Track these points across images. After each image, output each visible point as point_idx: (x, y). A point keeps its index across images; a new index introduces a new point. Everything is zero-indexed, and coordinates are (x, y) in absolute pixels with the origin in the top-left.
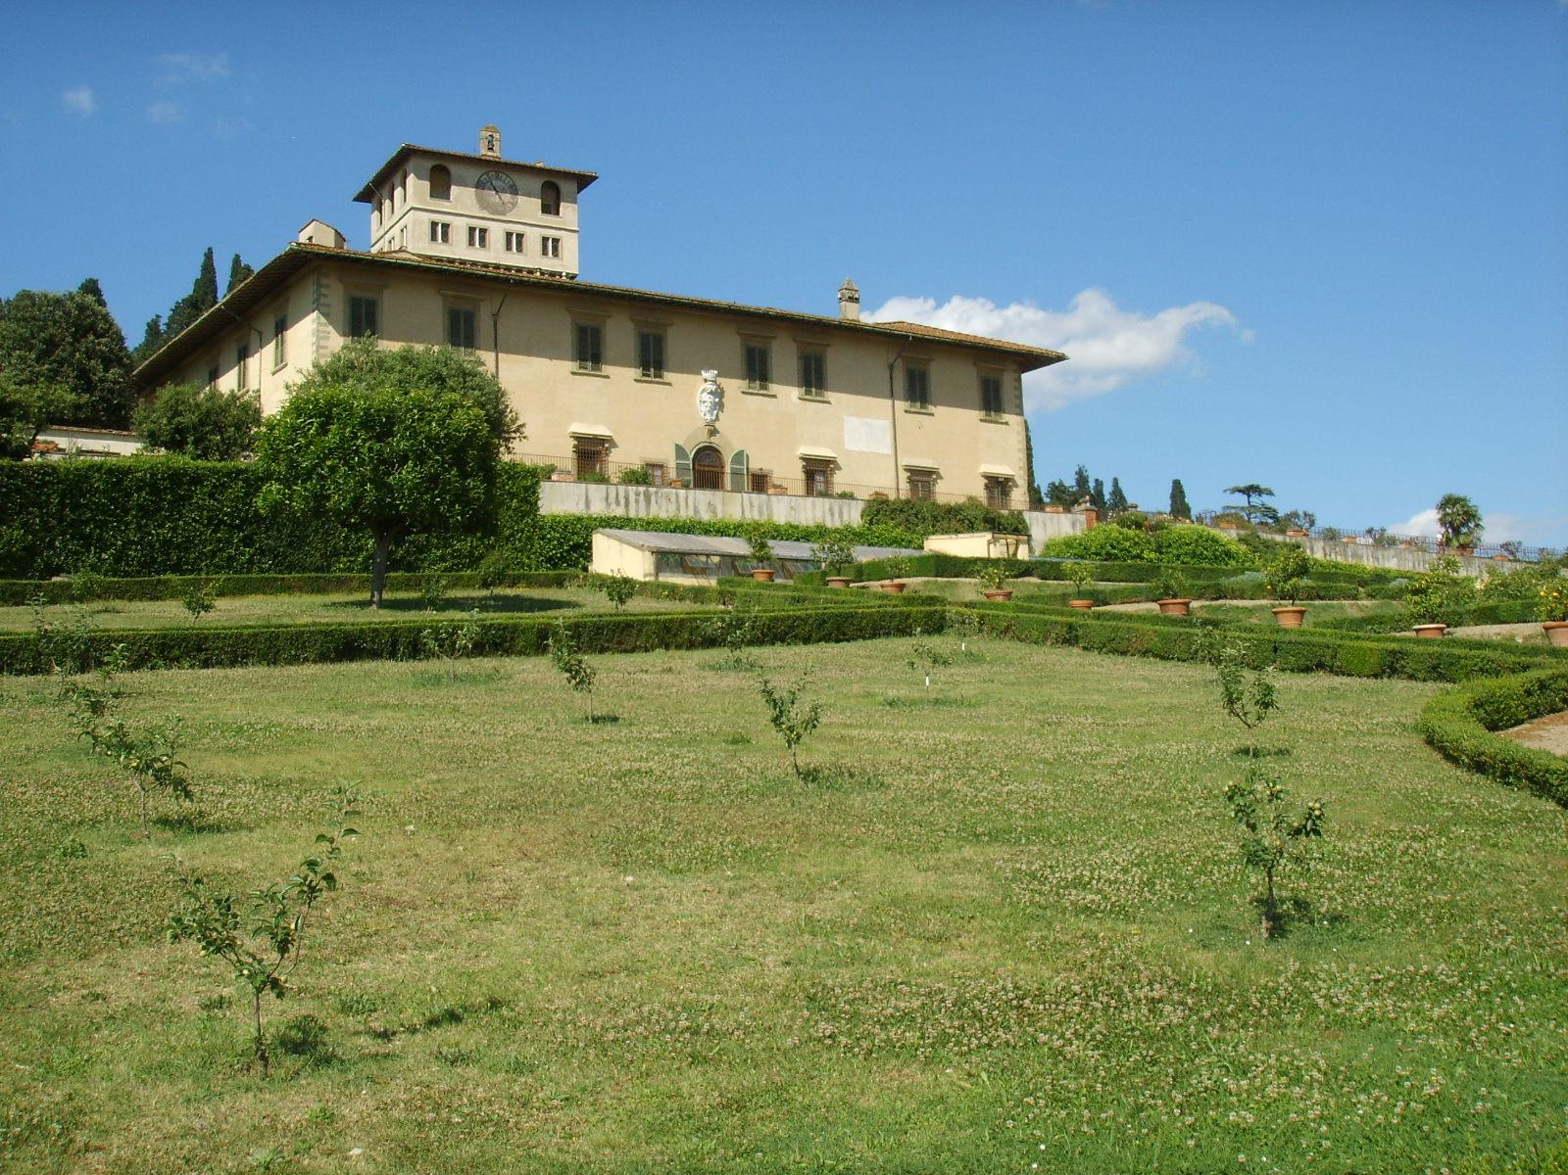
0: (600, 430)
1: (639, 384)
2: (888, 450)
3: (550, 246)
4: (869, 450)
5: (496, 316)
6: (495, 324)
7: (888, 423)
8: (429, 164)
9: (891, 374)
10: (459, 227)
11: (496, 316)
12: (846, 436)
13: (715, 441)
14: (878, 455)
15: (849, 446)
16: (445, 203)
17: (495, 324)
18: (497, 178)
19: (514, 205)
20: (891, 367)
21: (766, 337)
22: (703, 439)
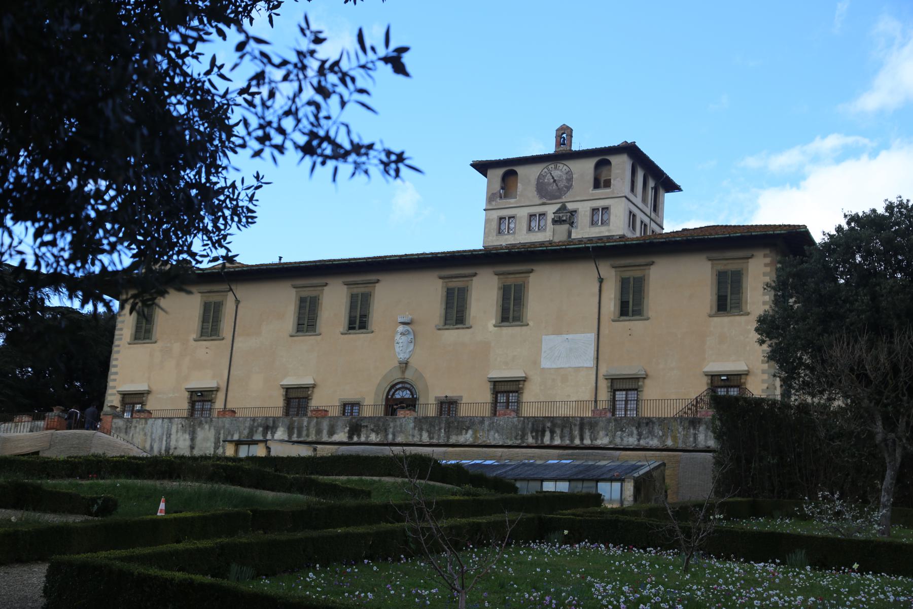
0: (308, 381)
1: (346, 336)
2: (591, 363)
3: (600, 214)
4: (567, 366)
5: (237, 302)
6: (237, 307)
7: (592, 336)
8: (500, 172)
9: (600, 287)
10: (523, 213)
11: (237, 302)
12: (543, 355)
13: (409, 375)
14: (577, 369)
15: (545, 364)
16: (512, 201)
17: (237, 307)
18: (556, 168)
19: (569, 188)
20: (601, 281)
21: (465, 276)
22: (397, 377)
